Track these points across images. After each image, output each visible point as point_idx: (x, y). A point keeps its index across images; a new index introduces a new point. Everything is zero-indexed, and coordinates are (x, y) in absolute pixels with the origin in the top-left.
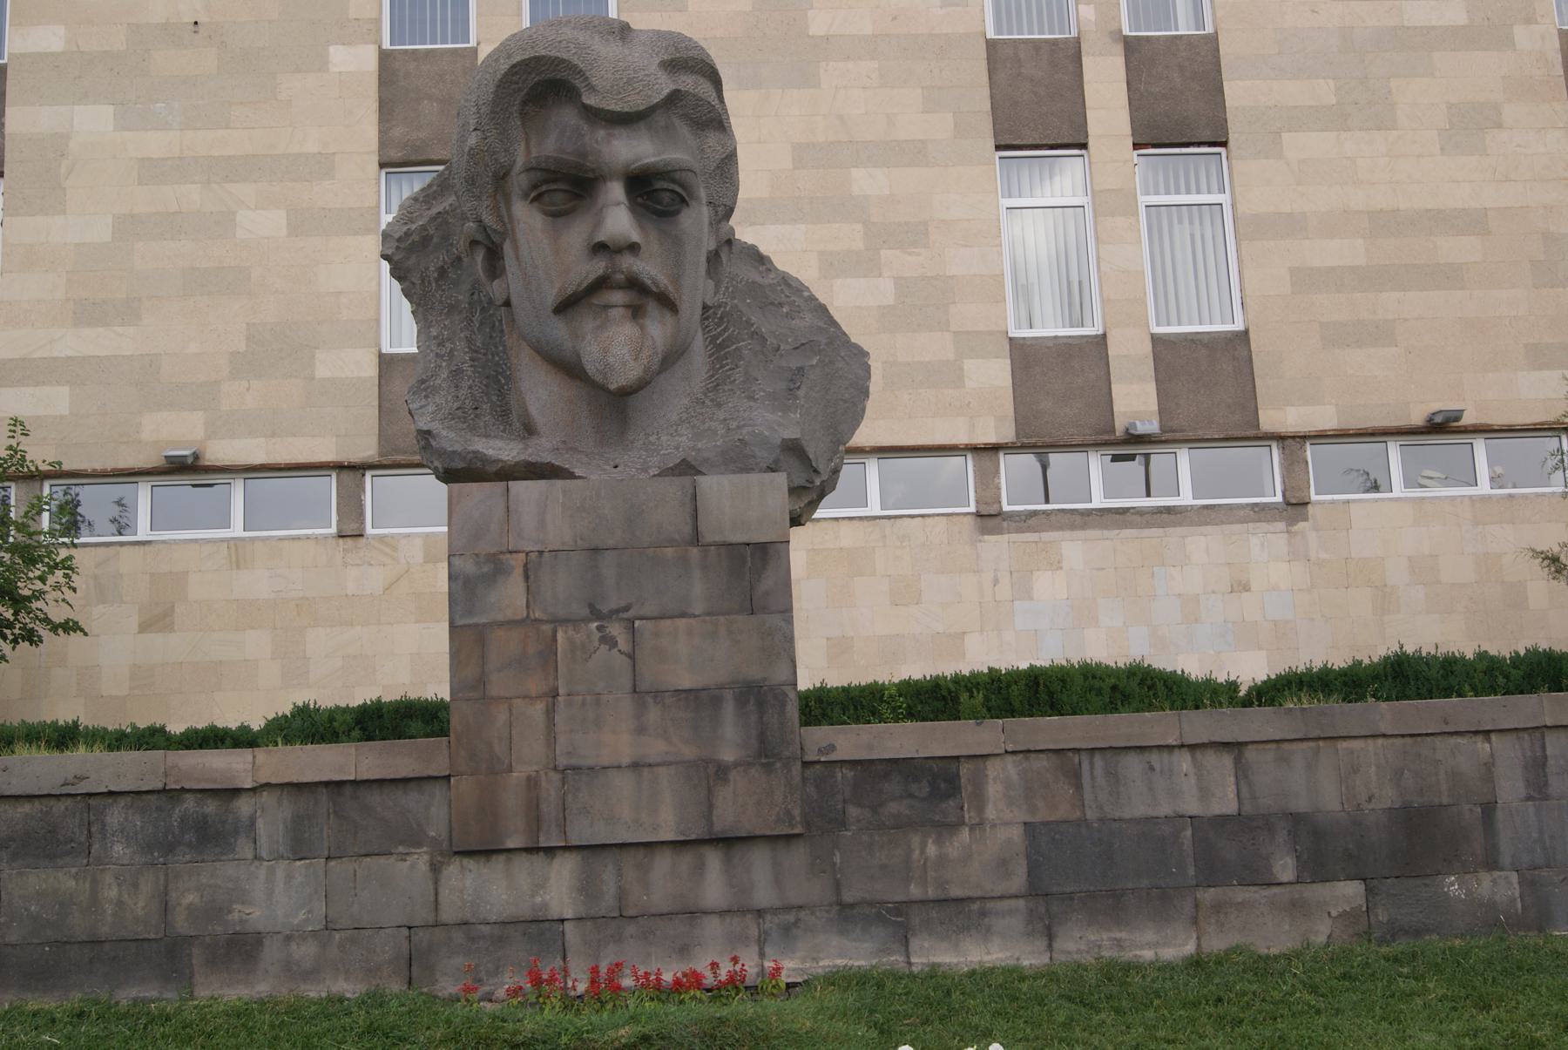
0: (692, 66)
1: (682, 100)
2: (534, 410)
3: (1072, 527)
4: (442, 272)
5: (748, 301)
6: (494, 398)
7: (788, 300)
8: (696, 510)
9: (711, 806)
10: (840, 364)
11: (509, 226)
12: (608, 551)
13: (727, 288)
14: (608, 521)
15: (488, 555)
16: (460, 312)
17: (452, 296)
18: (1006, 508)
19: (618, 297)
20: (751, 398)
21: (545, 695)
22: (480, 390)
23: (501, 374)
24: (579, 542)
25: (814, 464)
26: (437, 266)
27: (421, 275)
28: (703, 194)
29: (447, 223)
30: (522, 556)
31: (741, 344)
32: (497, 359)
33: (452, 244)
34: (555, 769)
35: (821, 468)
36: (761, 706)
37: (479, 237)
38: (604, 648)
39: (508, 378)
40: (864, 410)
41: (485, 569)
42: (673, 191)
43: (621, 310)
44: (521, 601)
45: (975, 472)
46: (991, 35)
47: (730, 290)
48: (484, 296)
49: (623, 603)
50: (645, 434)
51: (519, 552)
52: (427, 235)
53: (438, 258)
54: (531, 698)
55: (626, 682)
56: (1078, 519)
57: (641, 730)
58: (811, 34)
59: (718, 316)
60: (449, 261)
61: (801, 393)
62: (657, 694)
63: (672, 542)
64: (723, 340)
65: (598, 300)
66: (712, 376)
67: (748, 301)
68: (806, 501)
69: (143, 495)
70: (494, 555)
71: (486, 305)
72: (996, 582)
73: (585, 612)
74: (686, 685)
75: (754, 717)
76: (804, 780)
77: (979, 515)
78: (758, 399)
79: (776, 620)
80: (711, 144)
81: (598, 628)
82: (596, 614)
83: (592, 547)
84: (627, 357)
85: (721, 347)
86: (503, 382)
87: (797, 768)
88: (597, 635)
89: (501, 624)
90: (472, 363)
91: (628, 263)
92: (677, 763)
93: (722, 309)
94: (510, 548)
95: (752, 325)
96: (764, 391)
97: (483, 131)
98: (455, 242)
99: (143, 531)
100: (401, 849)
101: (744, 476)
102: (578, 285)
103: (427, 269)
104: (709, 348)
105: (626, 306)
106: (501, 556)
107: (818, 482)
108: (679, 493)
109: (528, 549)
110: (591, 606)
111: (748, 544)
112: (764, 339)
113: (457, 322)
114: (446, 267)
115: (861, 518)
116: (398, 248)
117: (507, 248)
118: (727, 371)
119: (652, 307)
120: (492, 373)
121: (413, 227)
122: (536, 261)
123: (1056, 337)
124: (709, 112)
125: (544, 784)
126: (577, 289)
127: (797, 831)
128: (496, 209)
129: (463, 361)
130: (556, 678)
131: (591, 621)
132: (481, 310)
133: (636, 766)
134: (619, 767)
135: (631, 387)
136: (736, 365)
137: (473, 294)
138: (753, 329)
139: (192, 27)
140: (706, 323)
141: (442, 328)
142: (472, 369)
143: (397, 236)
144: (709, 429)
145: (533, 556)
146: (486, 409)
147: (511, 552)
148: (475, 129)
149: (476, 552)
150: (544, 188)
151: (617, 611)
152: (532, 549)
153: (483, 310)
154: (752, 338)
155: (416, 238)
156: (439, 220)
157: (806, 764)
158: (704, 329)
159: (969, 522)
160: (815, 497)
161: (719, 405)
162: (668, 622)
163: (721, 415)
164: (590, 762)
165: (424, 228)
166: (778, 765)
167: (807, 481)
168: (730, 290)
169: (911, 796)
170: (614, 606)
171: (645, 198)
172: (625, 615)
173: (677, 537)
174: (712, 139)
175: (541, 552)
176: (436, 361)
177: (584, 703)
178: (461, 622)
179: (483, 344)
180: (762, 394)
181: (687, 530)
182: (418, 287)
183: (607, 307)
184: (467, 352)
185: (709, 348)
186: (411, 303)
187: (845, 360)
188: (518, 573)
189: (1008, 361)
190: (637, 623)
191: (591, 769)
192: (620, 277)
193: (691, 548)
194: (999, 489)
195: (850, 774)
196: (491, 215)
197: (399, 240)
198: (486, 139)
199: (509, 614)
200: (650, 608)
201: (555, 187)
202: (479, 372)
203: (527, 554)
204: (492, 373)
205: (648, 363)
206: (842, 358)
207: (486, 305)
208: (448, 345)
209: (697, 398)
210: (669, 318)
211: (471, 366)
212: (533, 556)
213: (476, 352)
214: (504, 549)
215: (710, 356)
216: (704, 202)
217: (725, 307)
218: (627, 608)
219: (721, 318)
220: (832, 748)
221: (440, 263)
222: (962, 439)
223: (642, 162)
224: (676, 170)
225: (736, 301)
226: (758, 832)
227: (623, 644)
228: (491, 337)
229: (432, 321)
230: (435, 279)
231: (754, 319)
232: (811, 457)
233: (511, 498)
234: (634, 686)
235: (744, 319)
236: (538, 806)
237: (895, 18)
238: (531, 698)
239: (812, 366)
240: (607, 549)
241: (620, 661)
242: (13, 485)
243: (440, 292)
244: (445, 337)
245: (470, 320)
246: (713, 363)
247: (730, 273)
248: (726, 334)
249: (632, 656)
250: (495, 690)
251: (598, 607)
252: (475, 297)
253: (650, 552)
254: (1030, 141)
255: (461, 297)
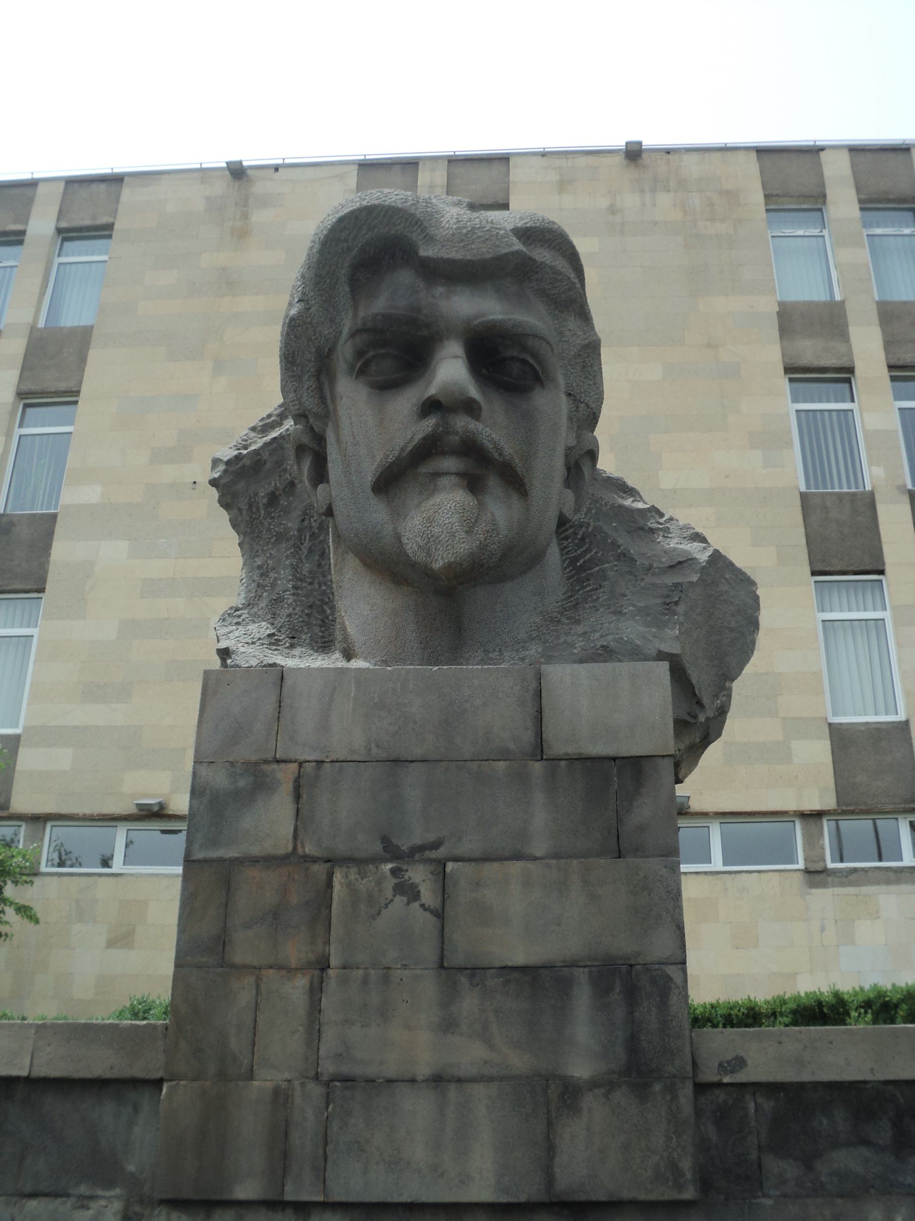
0: (550, 240)
1: (537, 273)
2: (352, 629)
3: (888, 882)
4: (273, 499)
5: (614, 524)
6: (317, 630)
7: (661, 527)
8: (540, 711)
9: (551, 1149)
10: (724, 587)
11: (331, 407)
12: (413, 764)
13: (590, 510)
14: (415, 722)
15: (247, 763)
16: (288, 539)
17: (281, 524)
18: (831, 865)
19: (450, 464)
20: (618, 613)
21: (310, 965)
22: (300, 619)
23: (326, 603)
24: (375, 751)
25: (697, 692)
26: (268, 491)
27: (250, 500)
28: (561, 380)
29: (282, 448)
30: (294, 767)
31: (605, 566)
32: (324, 588)
33: (285, 470)
34: (317, 1077)
35: (706, 701)
36: (632, 993)
37: (306, 440)
38: (400, 900)
39: (333, 608)
40: (753, 643)
41: (242, 783)
42: (524, 362)
43: (454, 479)
44: (287, 829)
45: (803, 835)
46: (803, 489)
47: (593, 511)
48: (315, 521)
49: (431, 837)
50: (485, 651)
51: (291, 762)
52: (260, 460)
53: (270, 484)
54: (289, 970)
55: (428, 951)
56: (891, 874)
57: (448, 1025)
58: (661, 487)
59: (579, 537)
60: (281, 487)
61: (681, 608)
62: (475, 972)
63: (505, 755)
64: (584, 562)
65: (426, 469)
66: (571, 596)
67: (614, 524)
68: (687, 743)
69: (120, 835)
70: (256, 764)
71: (316, 531)
72: (823, 929)
73: (378, 847)
74: (520, 958)
75: (620, 1012)
76: (698, 1112)
77: (807, 871)
78: (626, 613)
79: (654, 865)
80: (571, 327)
81: (395, 872)
82: (391, 851)
83: (392, 758)
84: (456, 527)
85: (583, 568)
86: (329, 612)
87: (686, 1092)
88: (390, 882)
89: (255, 861)
90: (295, 591)
91: (462, 423)
92: (502, 1079)
93: (584, 529)
94: (277, 757)
95: (619, 547)
96: (634, 606)
97: (308, 300)
98: (289, 467)
99: (117, 865)
100: (83, 1189)
101: (609, 666)
102: (402, 450)
103: (256, 494)
104: (568, 570)
105: (458, 474)
106: (266, 767)
107: (702, 718)
108: (518, 687)
109: (302, 758)
110: (386, 841)
111: (614, 759)
112: (633, 560)
113: (284, 550)
114: (277, 493)
115: (706, 873)
116: (225, 471)
117: (330, 437)
118: (589, 591)
119: (493, 481)
120: (317, 602)
121: (245, 452)
122: (357, 437)
123: (867, 723)
124: (569, 290)
125: (298, 1100)
126: (400, 454)
127: (689, 1194)
128: (320, 389)
129: (284, 589)
130: (327, 942)
131: (386, 861)
132: (310, 536)
133: (438, 1080)
134: (413, 1081)
135: (460, 564)
136: (601, 586)
137: (303, 520)
138: (619, 551)
139: (192, 486)
140: (565, 543)
141: (267, 557)
142: (295, 597)
143: (225, 459)
144: (565, 642)
145: (309, 768)
146: (305, 640)
147: (278, 762)
148: (299, 301)
149: (231, 759)
150: (371, 354)
151: (421, 849)
152: (308, 758)
153: (313, 536)
154: (619, 560)
155: (247, 462)
156: (274, 445)
157: (701, 1088)
158: (562, 550)
159: (799, 878)
160: (698, 740)
161: (578, 622)
162: (496, 865)
163: (580, 629)
164: (371, 1071)
165: (256, 452)
166: (657, 1087)
167: (689, 714)
168: (593, 511)
169: (865, 1142)
170: (417, 840)
171: (491, 369)
172: (434, 854)
173: (512, 746)
174: (572, 323)
175: (320, 763)
176: (256, 591)
177: (365, 981)
178: (199, 855)
179: (310, 572)
180: (631, 608)
181: (528, 736)
182: (245, 513)
183: (437, 475)
184: (290, 580)
185: (568, 570)
186: (238, 533)
187: (730, 584)
188: (286, 788)
189: (828, 742)
190: (450, 866)
191: (370, 1081)
192: (454, 439)
193: (531, 762)
194: (823, 849)
195: (768, 1105)
196: (312, 397)
197: (228, 463)
198: (310, 309)
199: (269, 847)
200: (470, 845)
201: (383, 351)
202: (301, 601)
203: (301, 765)
204: (317, 602)
205: (485, 539)
206: (727, 580)
207: (316, 531)
208: (273, 575)
209: (551, 617)
210: (516, 503)
211: (294, 594)
212: (309, 768)
213: (301, 580)
214: (270, 756)
215: (569, 578)
216: (562, 387)
217: (587, 528)
218: (436, 845)
219: (583, 539)
220: (739, 1063)
221: (271, 489)
222: (791, 806)
223: (486, 319)
224: (529, 335)
225: (600, 523)
226: (626, 1195)
227: (428, 895)
228: (320, 565)
229: (257, 551)
230: (264, 505)
231: (620, 541)
232: (694, 681)
233: (285, 689)
234: (442, 958)
235: (609, 541)
236: (286, 1134)
237: (727, 477)
238: (289, 970)
239: (691, 583)
240: (413, 761)
241: (423, 922)
242: (24, 825)
243: (268, 520)
244: (270, 566)
245: (298, 548)
246: (571, 584)
247: (593, 495)
248: (588, 556)
249: (440, 914)
250: (240, 955)
251: (395, 841)
252: (306, 523)
253: (474, 766)
254: (839, 568)
255: (290, 524)
